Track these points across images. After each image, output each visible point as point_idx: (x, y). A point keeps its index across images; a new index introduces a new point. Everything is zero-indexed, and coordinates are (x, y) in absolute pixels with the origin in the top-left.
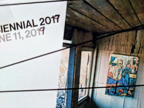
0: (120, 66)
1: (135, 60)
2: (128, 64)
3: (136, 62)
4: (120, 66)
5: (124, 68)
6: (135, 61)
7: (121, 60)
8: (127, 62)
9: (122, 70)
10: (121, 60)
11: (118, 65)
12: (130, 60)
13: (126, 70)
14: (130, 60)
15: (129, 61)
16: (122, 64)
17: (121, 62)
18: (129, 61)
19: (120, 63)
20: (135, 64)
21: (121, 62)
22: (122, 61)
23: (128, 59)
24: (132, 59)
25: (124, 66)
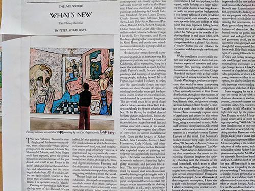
0: (39, 92)
1: (98, 59)
2: (73, 77)
3: (104, 67)
4: (39, 92)
5: (58, 96)
6: (99, 63)
7: (44, 67)
8: (67, 70)
9: (50, 105)
10: (44, 67)
11: (35, 81)
12: (78, 59)
13: (66, 103)
14: (78, 59)
15: (75, 67)
16: (48, 80)
17: (43, 74)
18: (75, 67)
19: (40, 79)
20: (100, 79)
21: (43, 74)
22: (49, 71)
23: (70, 59)
24: (88, 57)
25: (60, 88)
